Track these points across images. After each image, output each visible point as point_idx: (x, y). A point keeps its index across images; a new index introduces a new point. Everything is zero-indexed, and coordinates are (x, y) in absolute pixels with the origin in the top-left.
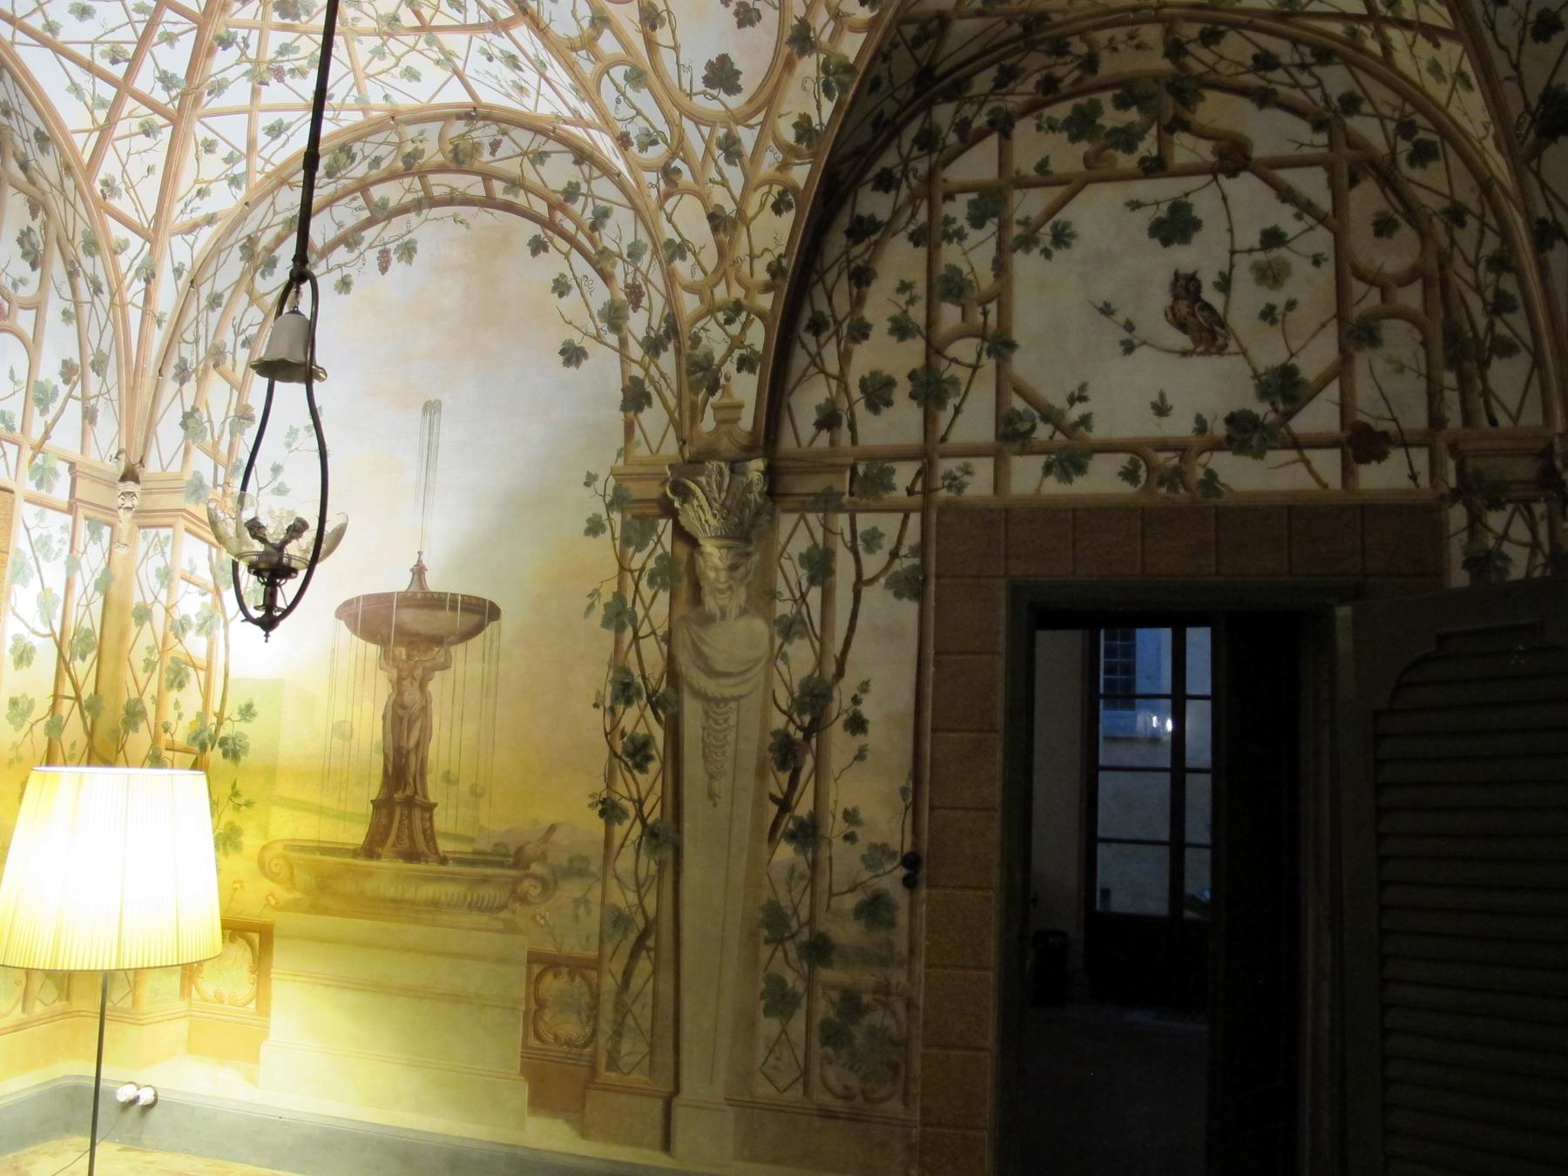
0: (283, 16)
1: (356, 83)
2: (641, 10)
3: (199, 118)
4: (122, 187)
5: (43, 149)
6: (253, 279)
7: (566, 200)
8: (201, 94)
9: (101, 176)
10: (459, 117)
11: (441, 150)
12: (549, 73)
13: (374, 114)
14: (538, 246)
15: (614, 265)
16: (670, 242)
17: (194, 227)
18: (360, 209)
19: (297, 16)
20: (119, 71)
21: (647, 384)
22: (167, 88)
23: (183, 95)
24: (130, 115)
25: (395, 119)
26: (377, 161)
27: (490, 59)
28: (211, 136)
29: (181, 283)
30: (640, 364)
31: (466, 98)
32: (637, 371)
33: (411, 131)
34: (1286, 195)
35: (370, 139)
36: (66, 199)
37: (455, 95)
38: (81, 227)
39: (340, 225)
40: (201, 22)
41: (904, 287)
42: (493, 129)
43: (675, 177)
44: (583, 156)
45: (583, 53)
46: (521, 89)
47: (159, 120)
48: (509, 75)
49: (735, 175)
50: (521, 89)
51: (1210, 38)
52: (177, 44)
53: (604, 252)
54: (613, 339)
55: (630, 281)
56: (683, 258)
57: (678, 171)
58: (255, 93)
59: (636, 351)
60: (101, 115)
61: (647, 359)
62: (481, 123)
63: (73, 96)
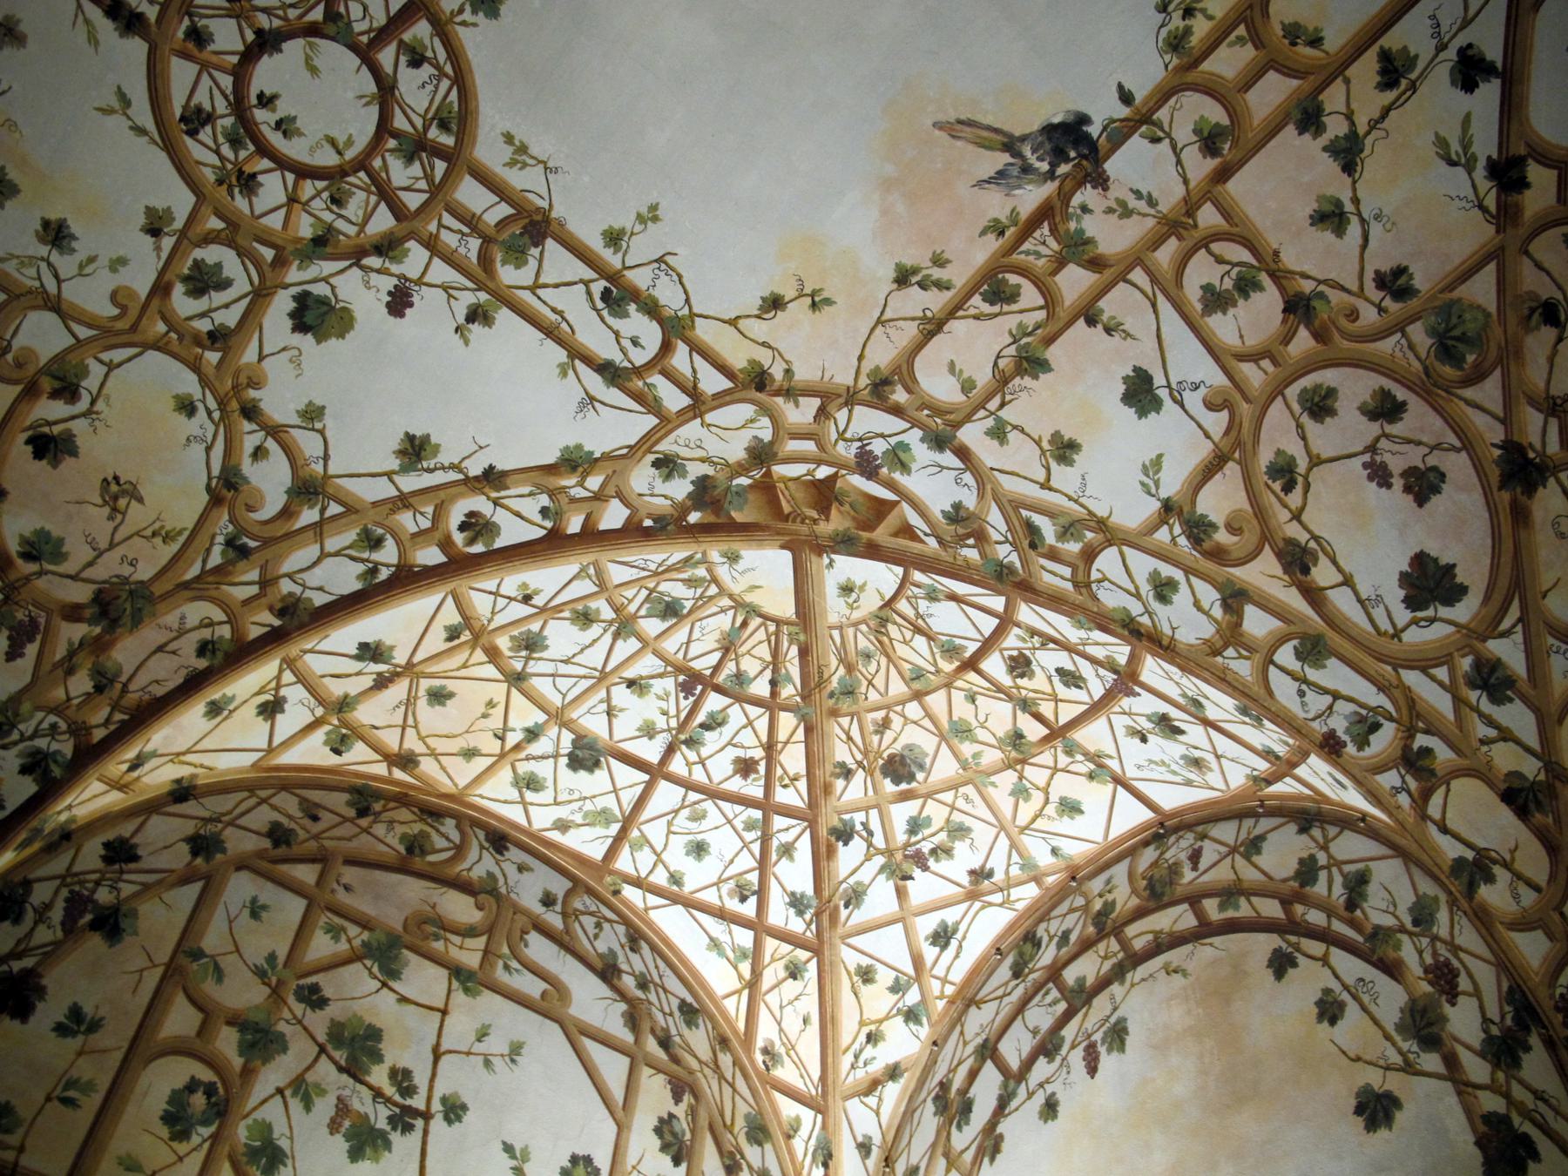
0: (896, 781)
1: (1013, 845)
2: (1279, 555)
3: (843, 938)
4: (782, 1050)
5: (690, 1023)
6: (949, 1134)
7: (1302, 886)
8: (836, 908)
9: (760, 1044)
10: (1146, 843)
11: (1134, 891)
12: (1212, 713)
13: (1050, 880)
14: (1281, 964)
15: (1398, 947)
16: (1459, 863)
17: (873, 1085)
18: (1055, 1002)
19: (911, 777)
20: (749, 909)
21: (1516, 1120)
22: (800, 913)
23: (818, 914)
24: (773, 960)
25: (1076, 876)
26: (1065, 937)
27: (1144, 740)
28: (865, 961)
29: (872, 1162)
30: (1492, 1087)
31: (1146, 815)
32: (1490, 1103)
33: (1097, 885)
35: (1054, 914)
36: (722, 1077)
37: (1131, 816)
38: (743, 1109)
39: (1035, 1032)
40: (809, 816)
42: (1188, 840)
43: (1426, 763)
44: (1310, 816)
45: (1230, 652)
46: (1197, 763)
47: (803, 955)
48: (1173, 750)
49: (1517, 717)
50: (1197, 763)
52: (796, 855)
53: (1378, 935)
54: (1431, 1061)
55: (1429, 960)
56: (1490, 879)
57: (1427, 752)
58: (901, 893)
59: (1477, 1069)
60: (745, 968)
61: (1501, 1076)
62: (1173, 839)
63: (714, 955)
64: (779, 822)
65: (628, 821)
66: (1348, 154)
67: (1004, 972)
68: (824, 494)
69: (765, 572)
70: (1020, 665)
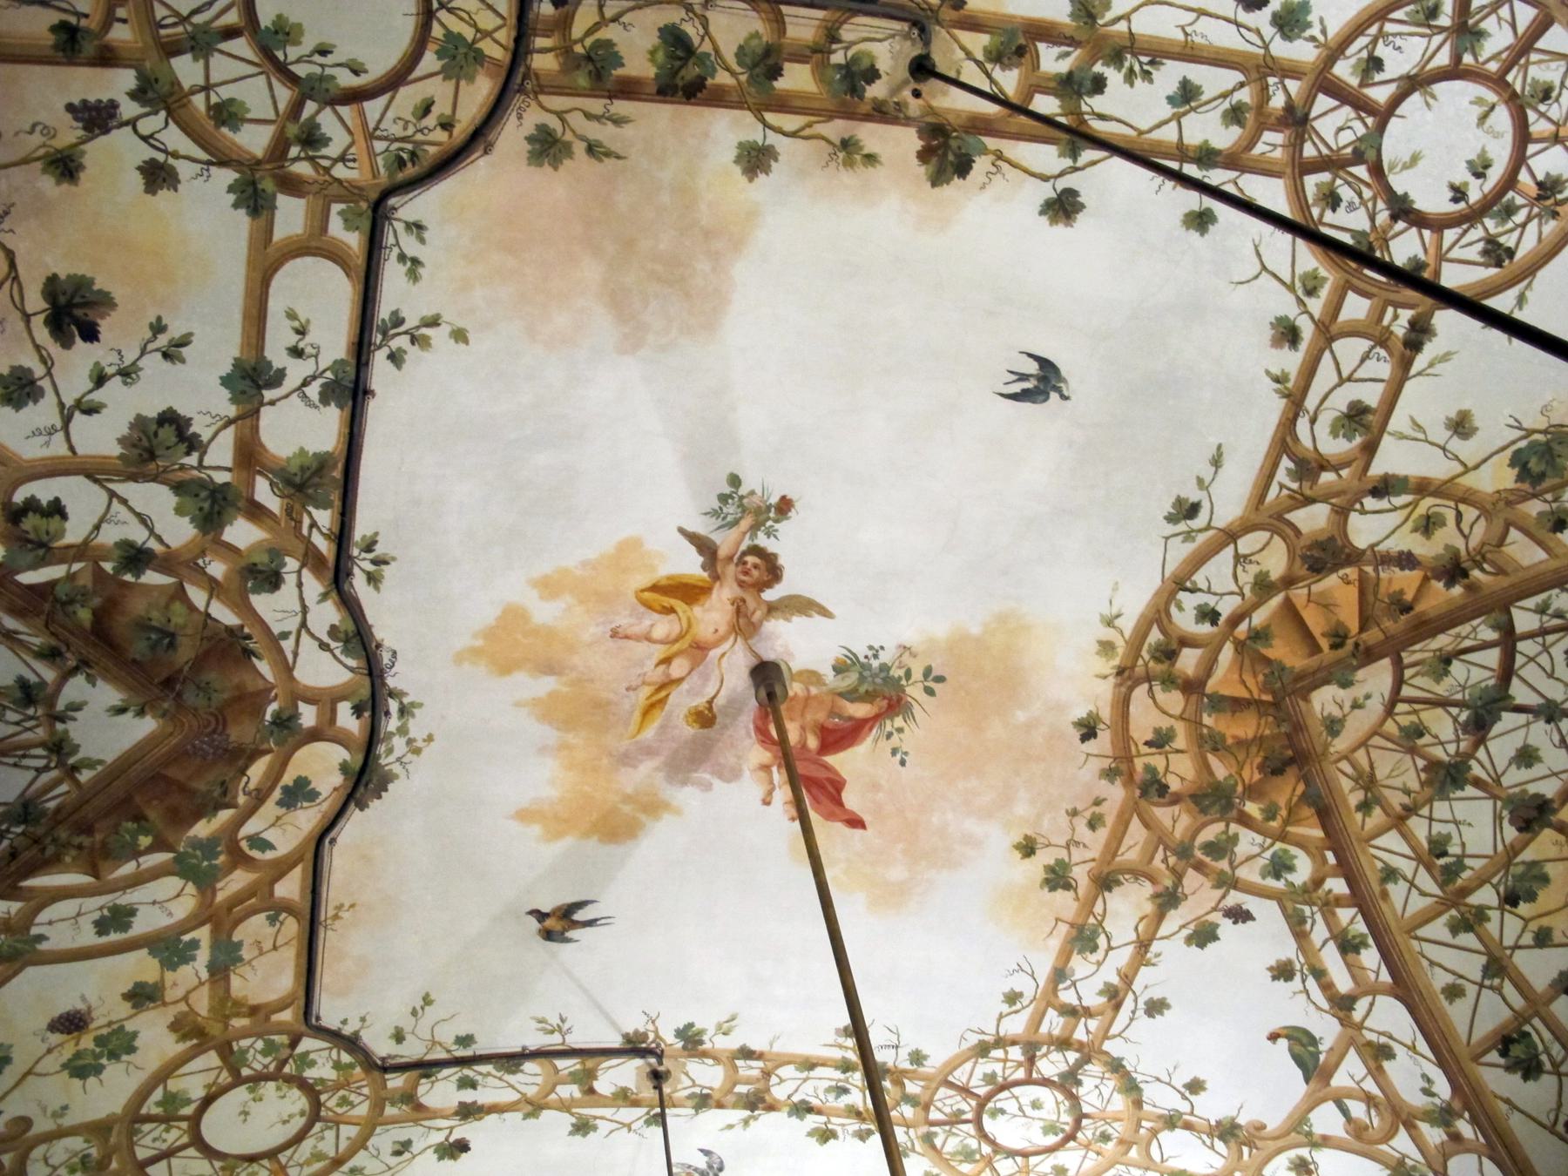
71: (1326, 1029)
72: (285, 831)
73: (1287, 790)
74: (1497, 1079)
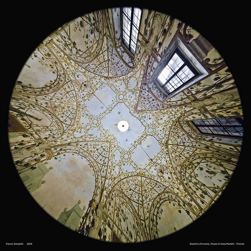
14: (170, 202)
33: (156, 199)
34: (204, 162)
40: (141, 194)
41: (193, 186)
51: (189, 160)
59: (184, 207)
64: (140, 195)
65: (132, 195)
66: (161, 160)
67: (152, 207)
68: (142, 174)
69: (139, 178)
70: (151, 184)
71: (92, 137)
72: (131, 109)
73: (106, 141)
74: (86, 143)
